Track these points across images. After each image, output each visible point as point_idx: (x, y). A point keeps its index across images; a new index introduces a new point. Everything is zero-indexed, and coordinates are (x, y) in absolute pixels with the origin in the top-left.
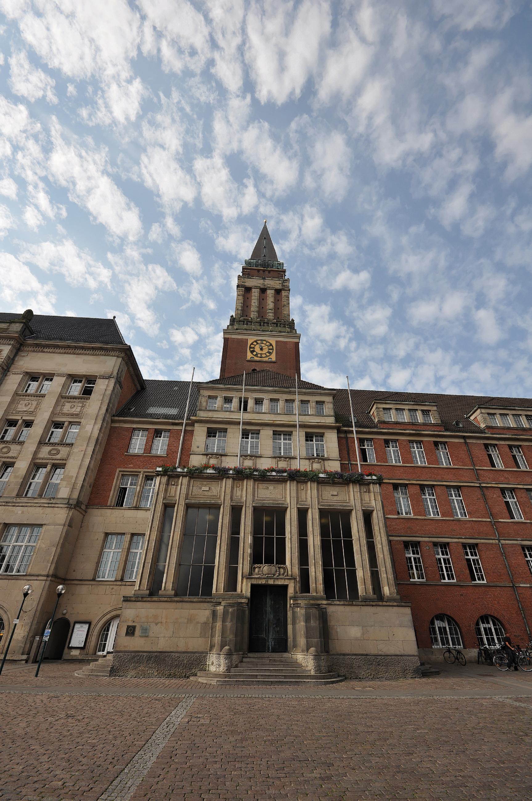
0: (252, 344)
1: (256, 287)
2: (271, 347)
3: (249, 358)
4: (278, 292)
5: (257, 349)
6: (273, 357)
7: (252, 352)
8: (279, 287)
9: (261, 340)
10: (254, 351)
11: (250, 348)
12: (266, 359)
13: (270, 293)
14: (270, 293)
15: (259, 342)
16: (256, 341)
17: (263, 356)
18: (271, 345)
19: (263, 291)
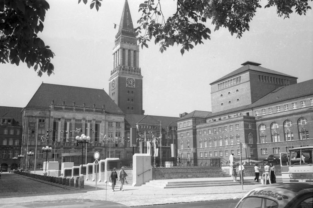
0: (127, 80)
1: (127, 49)
2: (133, 82)
3: (127, 86)
4: (135, 51)
5: (129, 83)
6: (134, 86)
7: (128, 83)
8: (135, 49)
9: (130, 78)
10: (128, 83)
11: (127, 82)
12: (132, 87)
13: (132, 52)
14: (132, 52)
15: (130, 79)
16: (129, 79)
17: (131, 85)
18: (134, 81)
19: (129, 50)
